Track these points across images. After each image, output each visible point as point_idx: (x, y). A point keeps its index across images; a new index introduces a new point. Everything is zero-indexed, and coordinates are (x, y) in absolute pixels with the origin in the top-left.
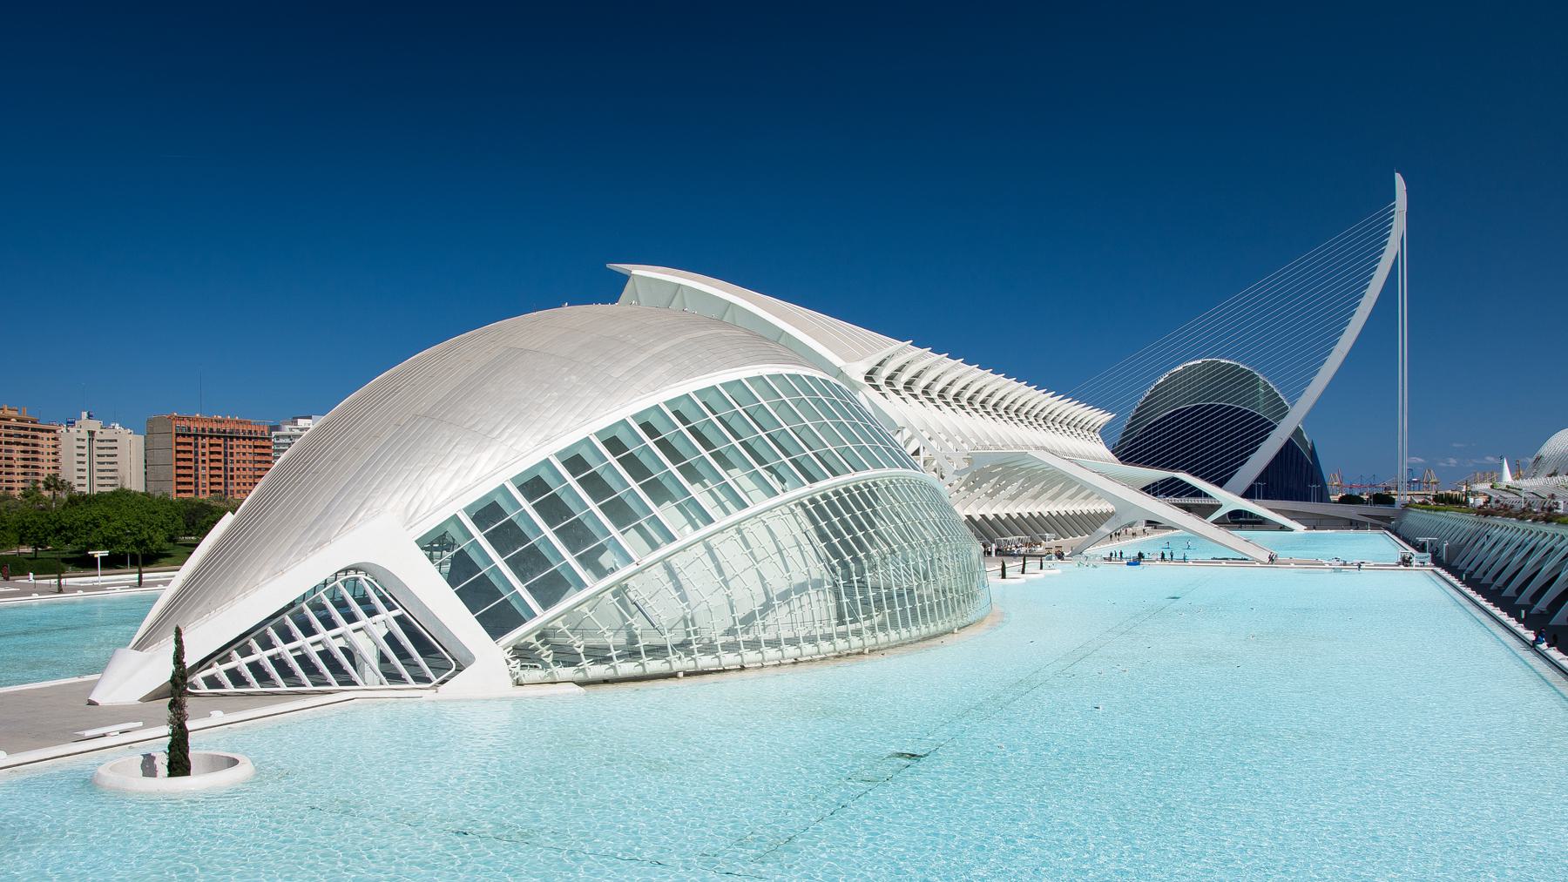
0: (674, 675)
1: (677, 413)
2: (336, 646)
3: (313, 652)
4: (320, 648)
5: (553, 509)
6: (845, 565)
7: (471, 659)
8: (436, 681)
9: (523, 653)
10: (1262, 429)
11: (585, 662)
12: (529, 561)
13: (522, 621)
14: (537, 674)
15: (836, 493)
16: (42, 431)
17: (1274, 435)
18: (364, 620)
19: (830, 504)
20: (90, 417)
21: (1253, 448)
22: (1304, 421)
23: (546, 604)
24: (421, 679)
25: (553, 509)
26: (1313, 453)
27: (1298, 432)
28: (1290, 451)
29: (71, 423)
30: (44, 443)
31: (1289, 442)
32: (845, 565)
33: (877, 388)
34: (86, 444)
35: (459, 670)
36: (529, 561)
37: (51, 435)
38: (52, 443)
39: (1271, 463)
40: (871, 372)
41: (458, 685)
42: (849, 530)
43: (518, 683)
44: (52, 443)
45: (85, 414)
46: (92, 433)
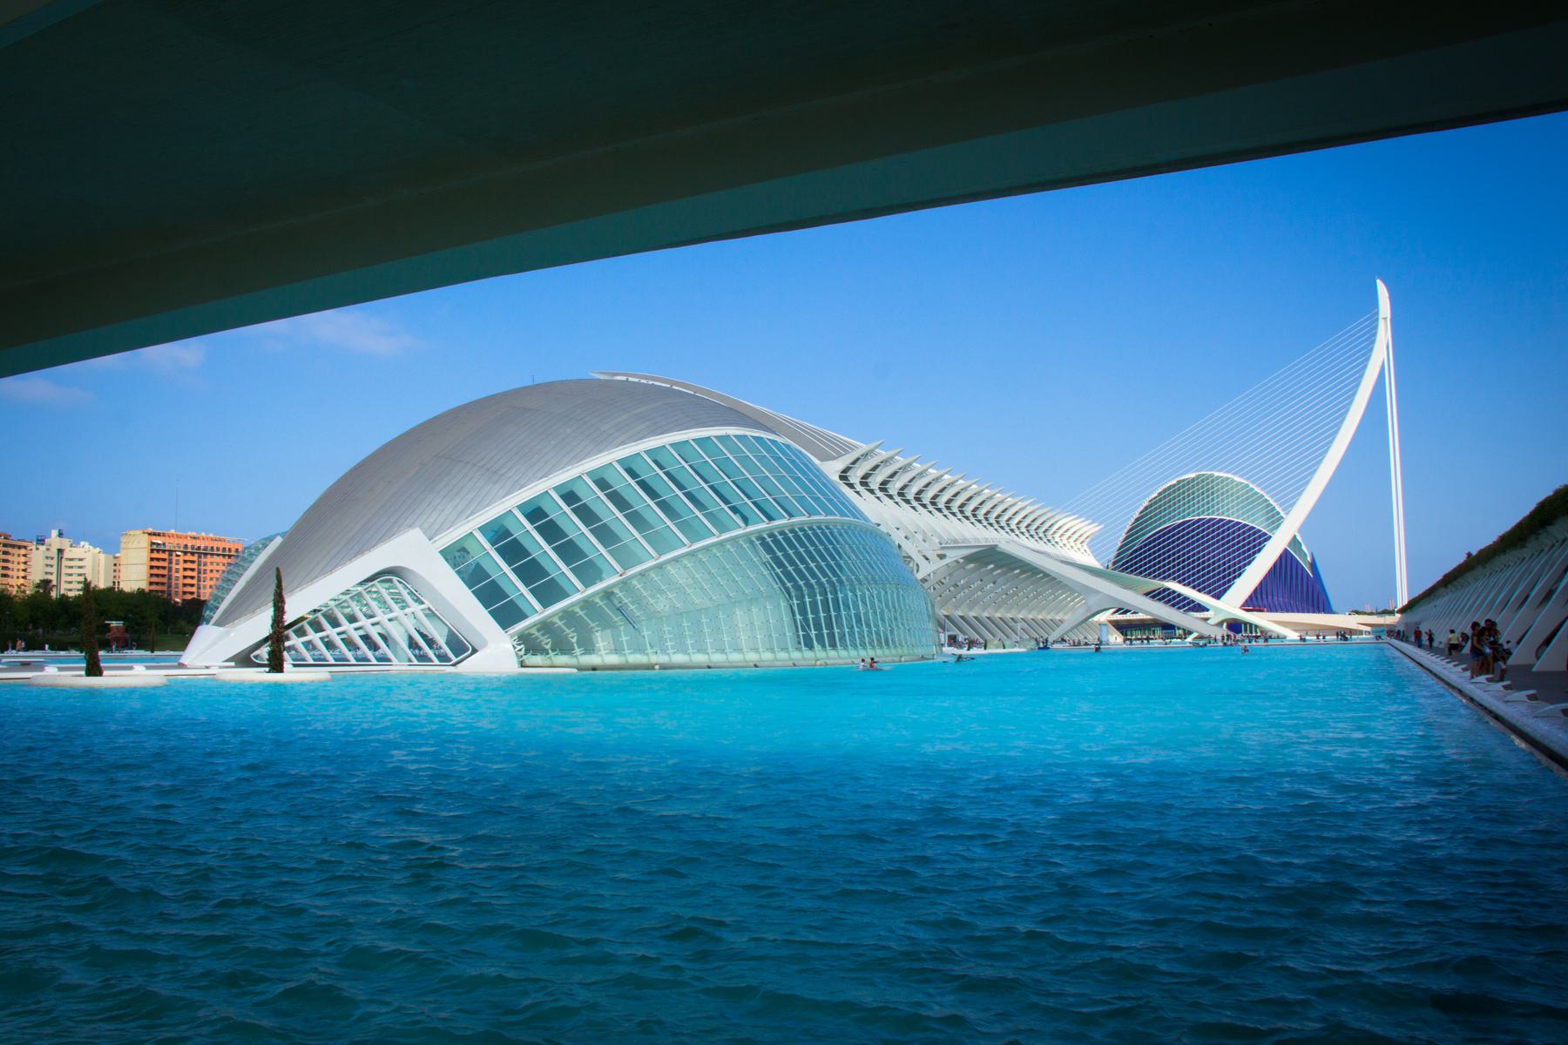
0: (651, 667)
1: (656, 462)
2: (374, 633)
3: (356, 637)
4: (362, 632)
5: (551, 531)
6: (797, 587)
7: (485, 644)
8: (455, 660)
9: (529, 644)
10: (1256, 541)
11: (578, 651)
12: (531, 572)
13: (525, 617)
14: (538, 659)
15: (792, 531)
16: (13, 546)
17: (1268, 544)
18: (397, 612)
19: (787, 539)
20: (61, 535)
21: (1248, 559)
22: (1300, 530)
23: (545, 605)
24: (443, 658)
25: (551, 531)
26: (1313, 565)
27: (1294, 542)
28: (1286, 563)
29: (41, 541)
30: (15, 559)
31: (1285, 554)
32: (797, 587)
33: (851, 486)
34: (55, 562)
35: (475, 651)
36: (531, 572)
37: (23, 551)
38: (23, 559)
39: (1265, 578)
40: (846, 471)
41: (472, 666)
42: (803, 561)
43: (523, 665)
44: (23, 559)
45: (55, 533)
46: (60, 551)
